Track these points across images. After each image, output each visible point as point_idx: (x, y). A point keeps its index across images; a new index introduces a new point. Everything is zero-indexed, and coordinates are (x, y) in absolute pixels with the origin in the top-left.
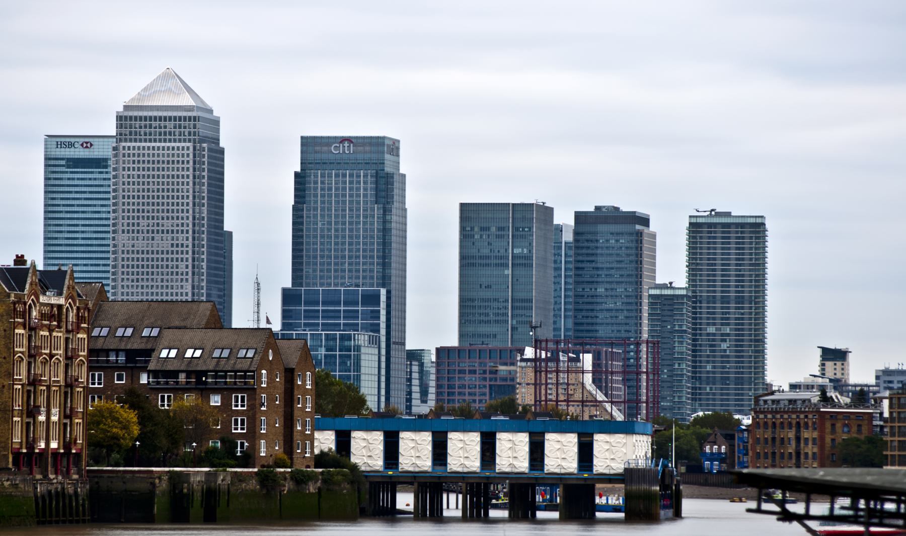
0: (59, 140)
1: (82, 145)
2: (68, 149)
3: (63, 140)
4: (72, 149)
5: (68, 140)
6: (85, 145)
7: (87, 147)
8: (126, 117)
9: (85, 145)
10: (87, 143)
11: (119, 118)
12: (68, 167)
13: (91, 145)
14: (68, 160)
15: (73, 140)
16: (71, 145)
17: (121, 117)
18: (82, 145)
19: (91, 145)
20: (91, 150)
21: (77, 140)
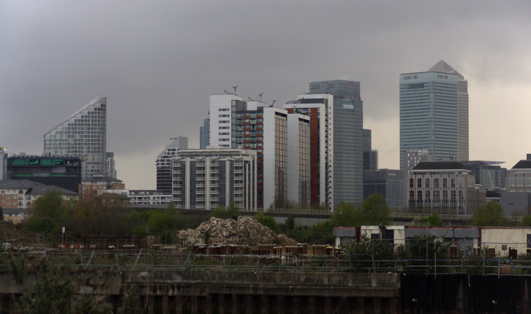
2: (408, 80)
3: (406, 76)
4: (410, 80)
5: (408, 75)
6: (415, 77)
7: (415, 78)
9: (415, 77)
10: (415, 76)
12: (408, 88)
13: (417, 77)
15: (410, 75)
16: (409, 78)
18: (414, 77)
19: (417, 77)
20: (417, 79)
21: (412, 75)
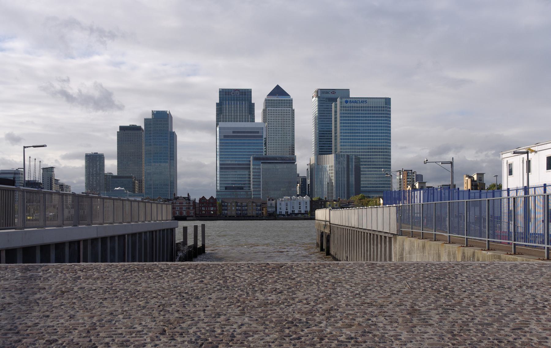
0: (322, 91)
1: (332, 93)
2: (326, 94)
3: (324, 91)
4: (328, 94)
5: (327, 91)
7: (333, 93)
8: (268, 100)
10: (333, 92)
11: (266, 100)
12: (326, 101)
13: (335, 93)
14: (327, 98)
15: (328, 91)
16: (327, 93)
17: (267, 100)
18: (332, 93)
19: (335, 93)
20: (335, 94)
21: (329, 91)
